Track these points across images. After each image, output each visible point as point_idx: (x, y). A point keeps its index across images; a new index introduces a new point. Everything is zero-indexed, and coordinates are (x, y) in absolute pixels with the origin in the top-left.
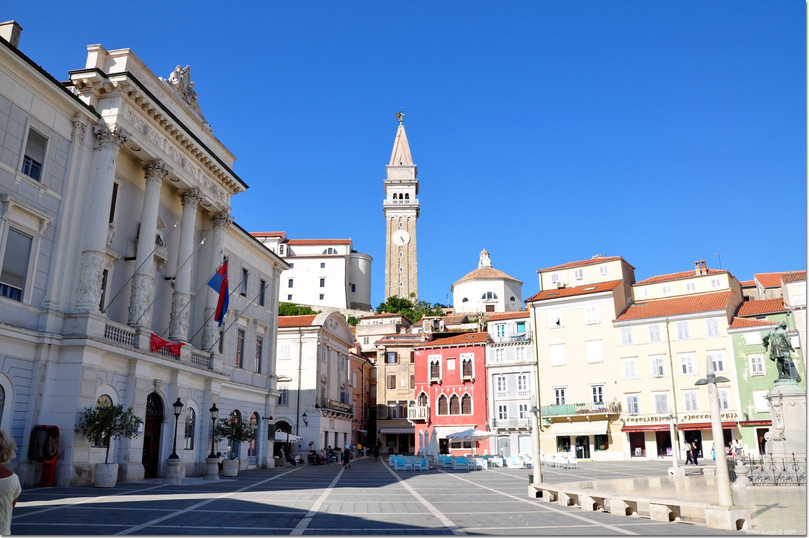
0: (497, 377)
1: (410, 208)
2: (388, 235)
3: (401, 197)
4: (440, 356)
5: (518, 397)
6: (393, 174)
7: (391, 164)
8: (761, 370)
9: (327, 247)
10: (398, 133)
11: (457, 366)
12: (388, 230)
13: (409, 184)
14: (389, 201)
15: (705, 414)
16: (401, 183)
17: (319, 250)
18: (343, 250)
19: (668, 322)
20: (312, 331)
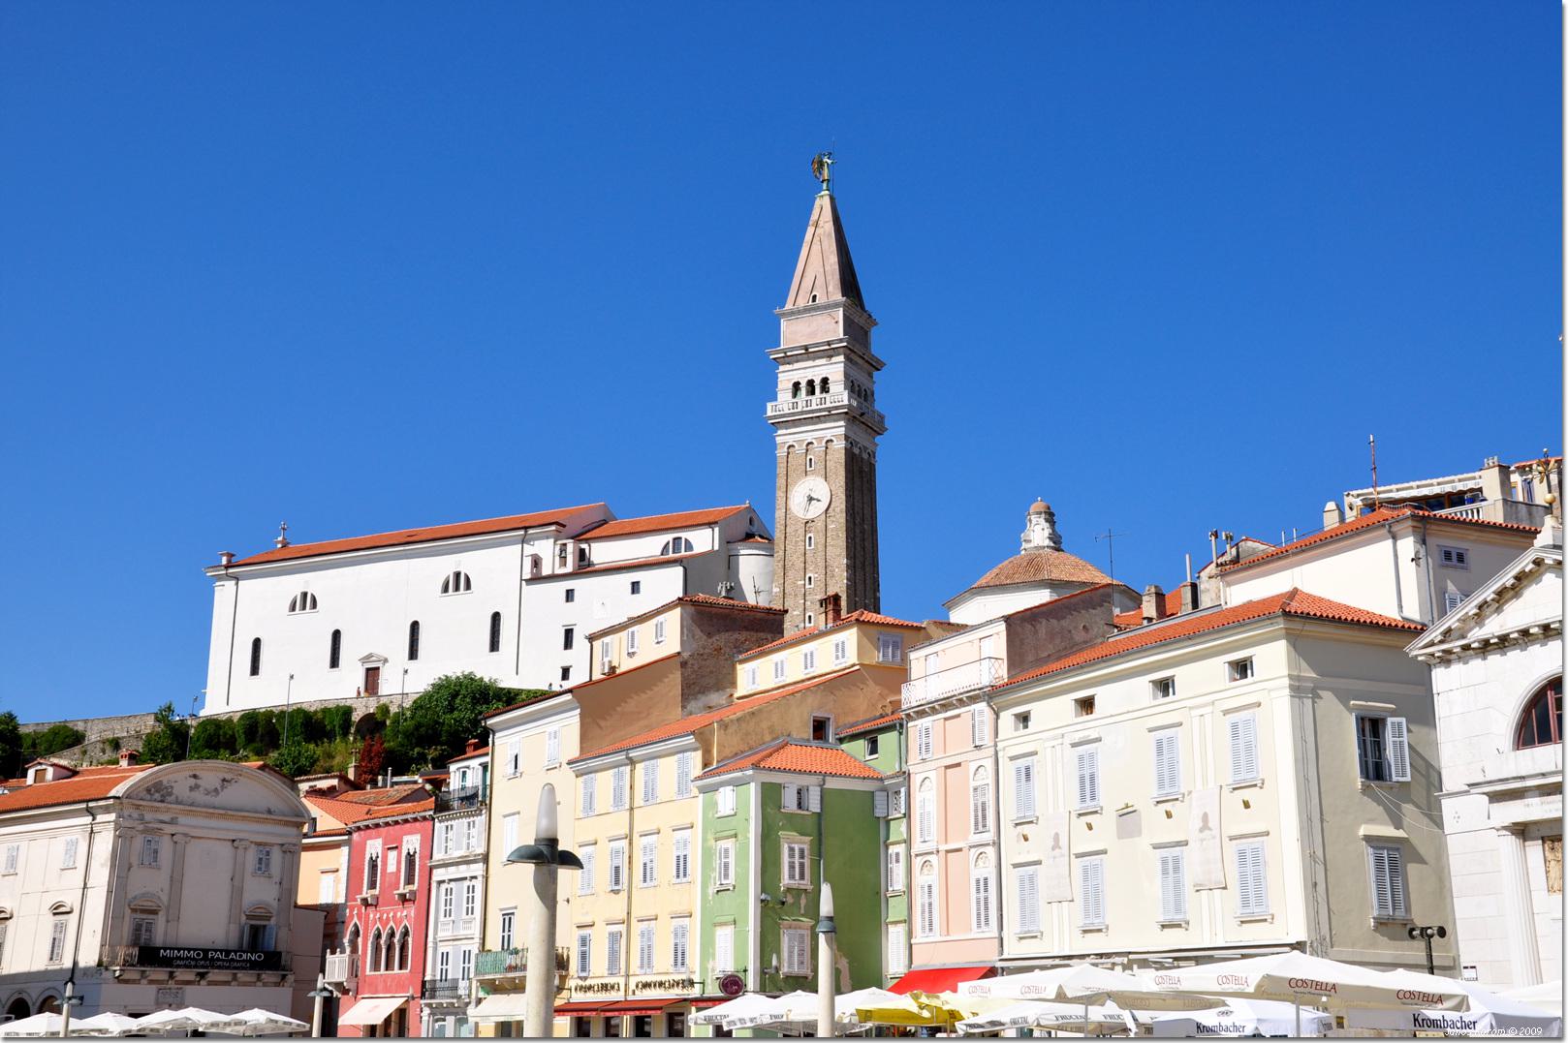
0: (444, 887)
1: (829, 415)
2: (780, 494)
3: (811, 383)
4: (379, 841)
5: (462, 933)
6: (793, 333)
7: (789, 306)
8: (726, 876)
9: (669, 537)
10: (814, 216)
11: (399, 863)
12: (781, 482)
13: (830, 354)
14: (783, 403)
15: (658, 978)
16: (808, 353)
17: (650, 546)
18: (703, 541)
19: (632, 762)
20: (107, 810)
